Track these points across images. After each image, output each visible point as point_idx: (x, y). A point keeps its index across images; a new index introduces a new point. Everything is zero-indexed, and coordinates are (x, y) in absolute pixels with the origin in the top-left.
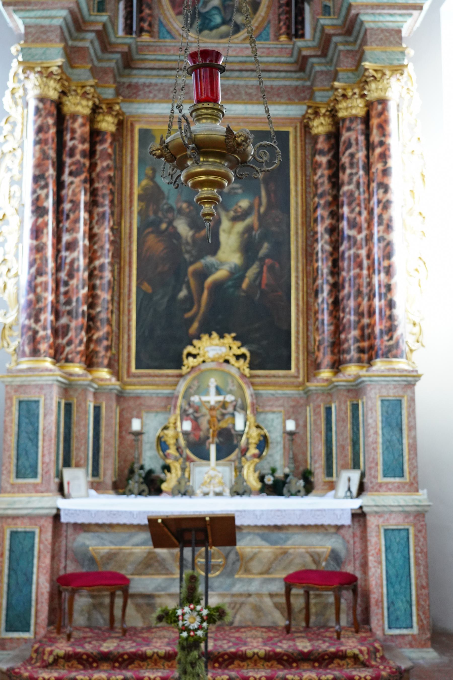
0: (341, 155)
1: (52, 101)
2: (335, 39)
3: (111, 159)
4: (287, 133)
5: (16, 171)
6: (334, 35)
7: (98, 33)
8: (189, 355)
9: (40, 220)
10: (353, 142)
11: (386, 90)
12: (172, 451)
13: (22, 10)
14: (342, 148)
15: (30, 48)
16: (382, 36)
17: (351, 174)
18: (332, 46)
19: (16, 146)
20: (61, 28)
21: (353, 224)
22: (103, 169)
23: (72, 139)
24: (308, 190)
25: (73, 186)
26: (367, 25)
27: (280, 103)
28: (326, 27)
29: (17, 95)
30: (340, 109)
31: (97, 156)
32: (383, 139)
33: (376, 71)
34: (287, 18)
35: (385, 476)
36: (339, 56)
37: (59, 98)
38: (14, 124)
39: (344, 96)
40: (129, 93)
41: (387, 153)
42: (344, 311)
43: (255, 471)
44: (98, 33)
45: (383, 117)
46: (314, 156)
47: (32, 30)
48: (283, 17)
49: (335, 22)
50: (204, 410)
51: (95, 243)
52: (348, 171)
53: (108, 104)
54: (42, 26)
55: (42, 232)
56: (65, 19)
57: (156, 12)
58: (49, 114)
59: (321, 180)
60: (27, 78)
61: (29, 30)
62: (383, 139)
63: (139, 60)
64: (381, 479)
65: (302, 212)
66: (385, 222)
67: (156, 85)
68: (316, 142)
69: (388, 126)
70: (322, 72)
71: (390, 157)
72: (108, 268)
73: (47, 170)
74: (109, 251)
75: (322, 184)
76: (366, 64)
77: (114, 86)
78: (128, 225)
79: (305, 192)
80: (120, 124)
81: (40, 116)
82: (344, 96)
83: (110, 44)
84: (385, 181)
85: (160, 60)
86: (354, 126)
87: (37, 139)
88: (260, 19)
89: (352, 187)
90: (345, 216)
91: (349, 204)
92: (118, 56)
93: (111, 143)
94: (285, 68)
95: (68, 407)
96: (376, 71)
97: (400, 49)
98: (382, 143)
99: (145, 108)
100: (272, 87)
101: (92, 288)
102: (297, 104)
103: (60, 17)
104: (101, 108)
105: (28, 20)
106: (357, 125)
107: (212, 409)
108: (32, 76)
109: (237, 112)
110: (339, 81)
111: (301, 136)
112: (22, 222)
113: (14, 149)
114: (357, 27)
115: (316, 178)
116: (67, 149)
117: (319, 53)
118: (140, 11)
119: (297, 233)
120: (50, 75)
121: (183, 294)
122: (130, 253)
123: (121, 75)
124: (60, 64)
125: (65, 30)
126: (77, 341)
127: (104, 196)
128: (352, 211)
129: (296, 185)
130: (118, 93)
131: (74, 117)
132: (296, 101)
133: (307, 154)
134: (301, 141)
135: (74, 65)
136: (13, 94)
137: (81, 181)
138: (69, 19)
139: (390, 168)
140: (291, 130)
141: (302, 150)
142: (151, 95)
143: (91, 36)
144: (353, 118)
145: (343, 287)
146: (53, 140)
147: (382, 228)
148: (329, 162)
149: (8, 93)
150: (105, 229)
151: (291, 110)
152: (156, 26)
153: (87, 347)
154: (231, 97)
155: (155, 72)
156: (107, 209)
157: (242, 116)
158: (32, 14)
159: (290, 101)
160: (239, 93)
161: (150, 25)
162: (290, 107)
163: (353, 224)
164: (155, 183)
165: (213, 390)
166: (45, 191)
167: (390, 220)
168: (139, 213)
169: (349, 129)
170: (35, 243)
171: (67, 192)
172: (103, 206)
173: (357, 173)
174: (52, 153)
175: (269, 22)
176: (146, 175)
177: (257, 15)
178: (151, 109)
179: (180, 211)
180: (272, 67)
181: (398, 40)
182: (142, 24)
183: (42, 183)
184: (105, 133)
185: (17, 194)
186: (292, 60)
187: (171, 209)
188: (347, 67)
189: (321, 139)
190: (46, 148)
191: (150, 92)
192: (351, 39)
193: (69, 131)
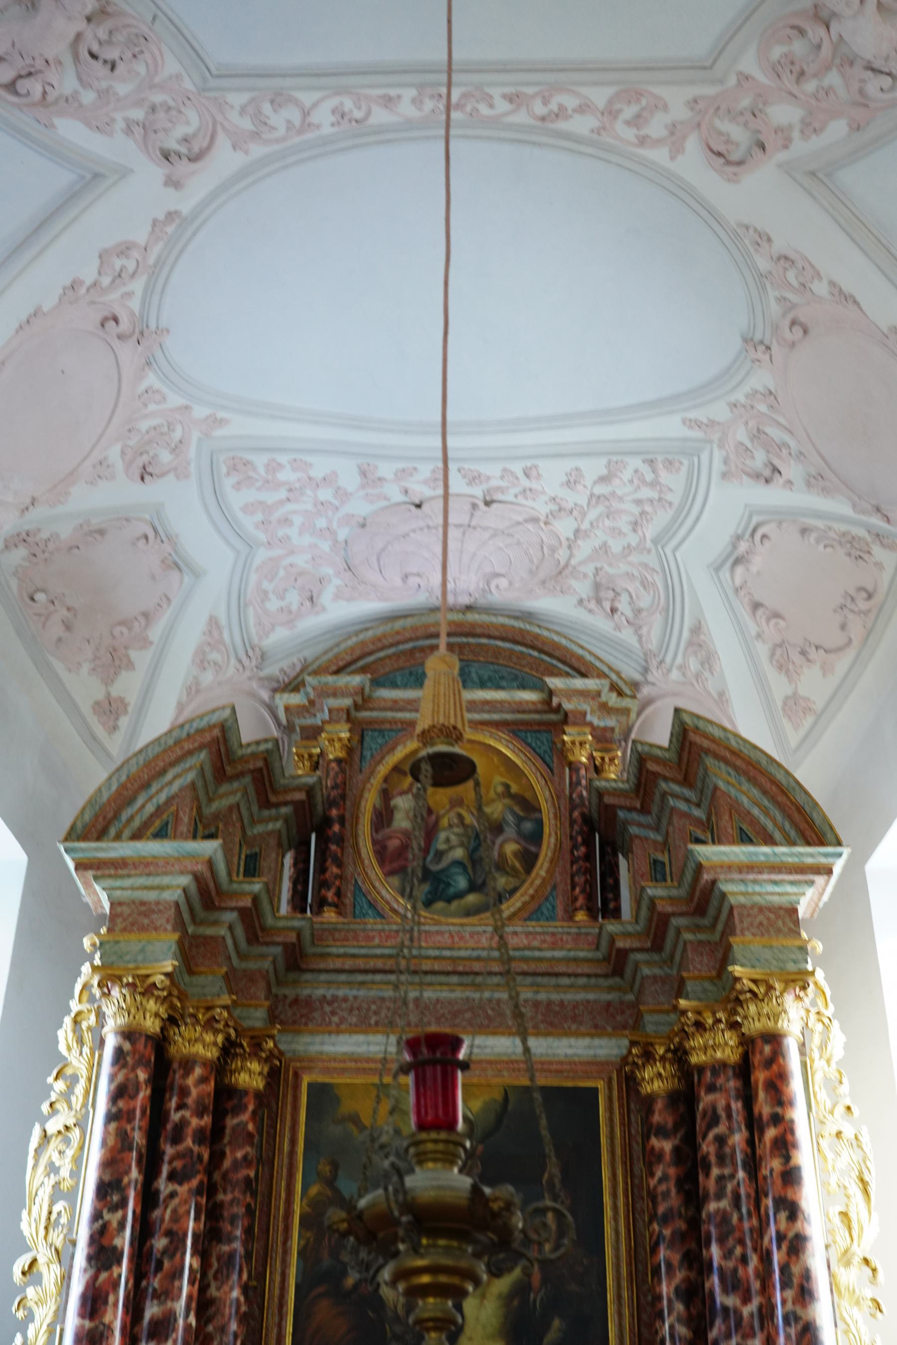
0: (699, 1139)
1: (148, 1037)
2: (675, 922)
3: (252, 1144)
4: (595, 1091)
5: (65, 1172)
6: (674, 914)
7: (244, 913)
9: (104, 1276)
11: (777, 1017)
13: (110, 876)
14: (700, 1124)
15: (117, 942)
16: (761, 918)
17: (721, 1179)
18: (671, 934)
19: (71, 1122)
20: (177, 904)
21: (732, 1283)
22: (236, 1165)
23: (180, 1107)
24: (638, 1206)
25: (176, 1201)
26: (733, 900)
27: (577, 1034)
28: (657, 902)
29: (84, 1025)
30: (694, 1048)
31: (226, 1140)
32: (779, 1110)
33: (754, 981)
34: (586, 881)
36: (685, 950)
37: (162, 1029)
38: (75, 1079)
39: (699, 1026)
40: (294, 1014)
41: (789, 1137)
44: (244, 913)
45: (775, 1067)
46: (646, 1138)
47: (126, 910)
48: (580, 879)
49: (674, 892)
51: (209, 1320)
52: (715, 1172)
53: (252, 1038)
54: (143, 903)
55: (106, 1302)
56: (185, 890)
57: (350, 869)
58: (141, 1062)
59: (663, 1188)
60: (107, 995)
61: (119, 909)
62: (779, 1110)
63: (314, 955)
65: (628, 1252)
66: (795, 1281)
67: (345, 999)
68: (650, 1111)
69: (787, 1085)
70: (655, 978)
71: (795, 1145)
73: (128, 1172)
74: (236, 1336)
75: (666, 1195)
76: (737, 970)
77: (267, 1003)
78: (278, 1278)
79: (633, 1210)
80: (274, 1076)
81: (124, 1066)
82: (699, 1026)
83: (263, 929)
84: (790, 1195)
85: (354, 956)
86: (720, 1081)
87: (114, 1110)
88: (538, 882)
89: (724, 1204)
90: (715, 1265)
91: (721, 1241)
92: (278, 950)
93: (254, 1113)
94: (586, 969)
96: (754, 981)
97: (797, 943)
98: (777, 1119)
99: (322, 1043)
100: (562, 1004)
102: (610, 1036)
103: (178, 886)
104: (241, 1046)
105: (118, 893)
106: (728, 1080)
108: (116, 992)
109: (496, 1050)
110: (687, 998)
111: (620, 1098)
112: (66, 1278)
113: (67, 1128)
114: (714, 902)
115: (653, 1182)
116: (169, 1127)
117: (649, 944)
118: (321, 869)
119: (619, 1297)
120: (149, 990)
123: (279, 983)
124: (169, 969)
125: (184, 908)
127: (233, 1220)
128: (727, 1254)
129: (614, 1195)
130: (273, 1017)
131: (188, 1064)
132: (609, 1029)
133: (633, 1132)
134: (621, 1106)
135: (195, 969)
136: (76, 1022)
137: (190, 1190)
138: (193, 890)
139: (797, 1169)
140: (600, 1085)
141: (622, 1124)
142: (335, 1019)
143: (230, 917)
144: (719, 1067)
146: (143, 1112)
147: (790, 1294)
148: (676, 1150)
149: (68, 1021)
150: (232, 1289)
151: (601, 1047)
154: (486, 1022)
155: (343, 977)
156: (237, 1245)
157: (505, 1058)
158: (128, 882)
159: (597, 1031)
160: (502, 1015)
161: (338, 894)
162: (597, 1042)
163: (732, 1283)
166: (120, 1214)
167: (807, 1275)
168: (299, 1253)
169: (712, 1088)
170: (87, 1324)
171: (163, 1215)
172: (230, 1239)
173: (733, 1176)
174: (138, 1138)
175: (554, 887)
176: (318, 1174)
177: (533, 874)
178: (334, 1044)
180: (561, 968)
181: (792, 926)
182: (323, 891)
184: (245, 1092)
185: (64, 1220)
186: (599, 955)
188: (700, 971)
189: (659, 1105)
190: (129, 1127)
191: (333, 1013)
192: (706, 922)
193: (176, 1091)
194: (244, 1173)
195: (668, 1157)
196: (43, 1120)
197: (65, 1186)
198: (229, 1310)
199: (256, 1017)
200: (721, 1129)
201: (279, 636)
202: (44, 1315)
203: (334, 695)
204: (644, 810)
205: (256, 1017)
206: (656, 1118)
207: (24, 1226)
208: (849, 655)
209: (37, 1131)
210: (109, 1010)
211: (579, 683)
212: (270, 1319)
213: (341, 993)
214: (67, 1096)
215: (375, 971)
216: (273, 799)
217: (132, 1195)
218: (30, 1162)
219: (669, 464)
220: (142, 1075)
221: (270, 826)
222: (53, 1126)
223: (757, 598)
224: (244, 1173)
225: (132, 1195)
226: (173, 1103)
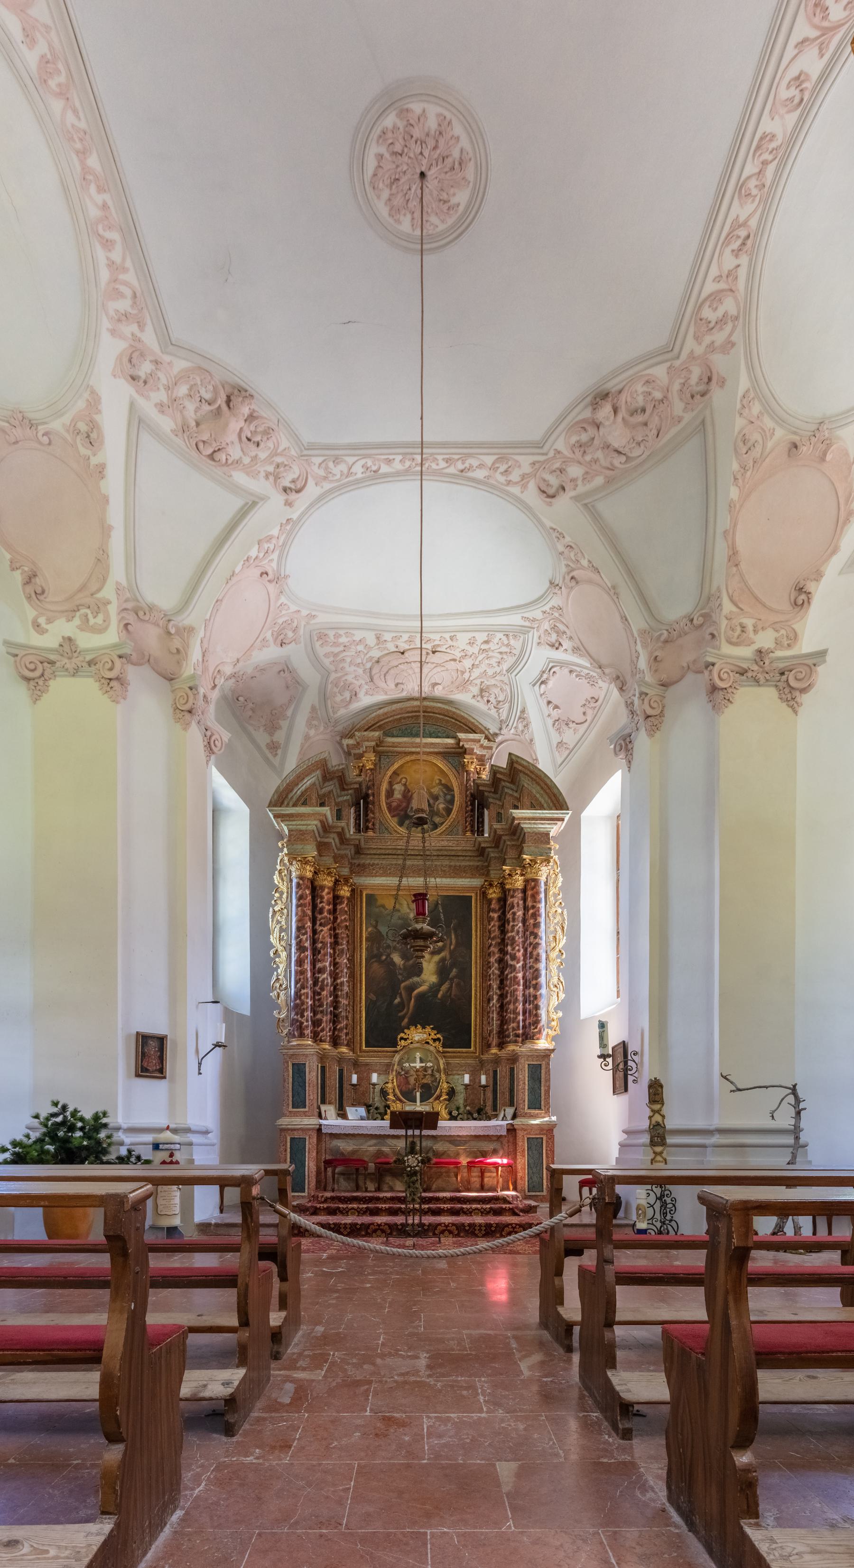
5: (283, 923)
12: (391, 1097)
27: (465, 877)
43: (446, 1108)
50: (412, 1072)
72: (346, 984)
75: (494, 931)
95: (323, 1069)
107: (417, 1071)
112: (289, 956)
118: (366, 815)
140: (473, 895)
148: (499, 917)
159: (473, 876)
165: (418, 1060)
189: (494, 902)
196: (273, 906)
197: (284, 927)
199: (345, 871)
202: (282, 967)
205: (345, 871)
206: (493, 906)
209: (271, 909)
213: (376, 862)
214: (280, 898)
221: (345, 798)
225: (308, 930)
226: (319, 901)
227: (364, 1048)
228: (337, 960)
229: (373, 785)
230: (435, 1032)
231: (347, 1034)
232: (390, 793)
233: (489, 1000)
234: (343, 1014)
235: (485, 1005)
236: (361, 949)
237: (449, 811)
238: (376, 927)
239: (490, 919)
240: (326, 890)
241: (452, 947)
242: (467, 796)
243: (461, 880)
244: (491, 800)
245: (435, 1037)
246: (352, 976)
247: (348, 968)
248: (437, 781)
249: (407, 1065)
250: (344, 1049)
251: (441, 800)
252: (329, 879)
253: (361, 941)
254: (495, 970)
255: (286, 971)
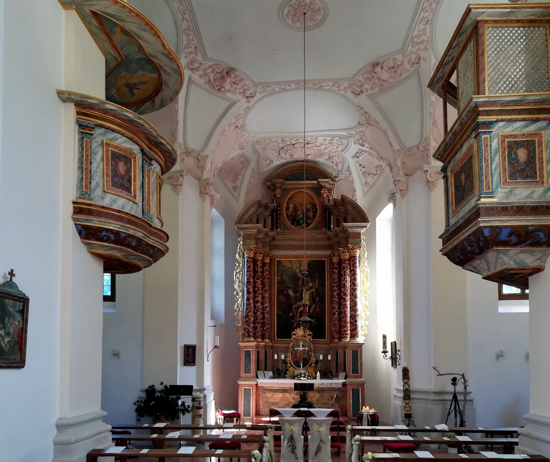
8: (293, 334)
10: (345, 267)
22: (266, 275)
23: (258, 267)
35: (353, 373)
38: (239, 264)
42: (342, 322)
52: (344, 277)
59: (335, 278)
64: (351, 374)
75: (336, 279)
80: (271, 259)
101: (263, 313)
121: (291, 314)
122: (274, 301)
126: (260, 332)
145: (342, 314)
152: (282, 225)
153: (262, 332)
156: (267, 288)
164: (282, 278)
165: (301, 346)
168: (277, 288)
169: (344, 263)
179: (290, 287)
183: (250, 284)
184: (266, 263)
187: (287, 287)
189: (336, 264)
194: (267, 276)
195: (336, 273)
198: (267, 298)
199: (267, 249)
200: (345, 270)
201: (266, 169)
203: (278, 184)
204: (336, 209)
207: (235, 287)
208: (377, 176)
210: (245, 253)
211: (325, 180)
212: (273, 298)
215: (287, 240)
216: (268, 209)
217: (252, 283)
218: (235, 277)
219: (344, 139)
220: (252, 264)
221: (268, 213)
222: (237, 271)
223: (360, 163)
224: (267, 276)
227: (276, 339)
228: (264, 295)
229: (280, 205)
230: (309, 331)
231: (268, 332)
232: (287, 209)
233: (334, 314)
234: (267, 322)
235: (332, 316)
236: (275, 288)
237: (314, 217)
238: (281, 277)
239: (334, 273)
240: (260, 261)
241: (316, 287)
242: (323, 209)
243: (320, 252)
244: (334, 212)
245: (309, 333)
246: (270, 302)
247: (269, 299)
248: (309, 202)
249: (296, 349)
250: (267, 340)
251: (311, 211)
252: (261, 256)
253: (275, 284)
254: (336, 299)
255: (241, 302)
